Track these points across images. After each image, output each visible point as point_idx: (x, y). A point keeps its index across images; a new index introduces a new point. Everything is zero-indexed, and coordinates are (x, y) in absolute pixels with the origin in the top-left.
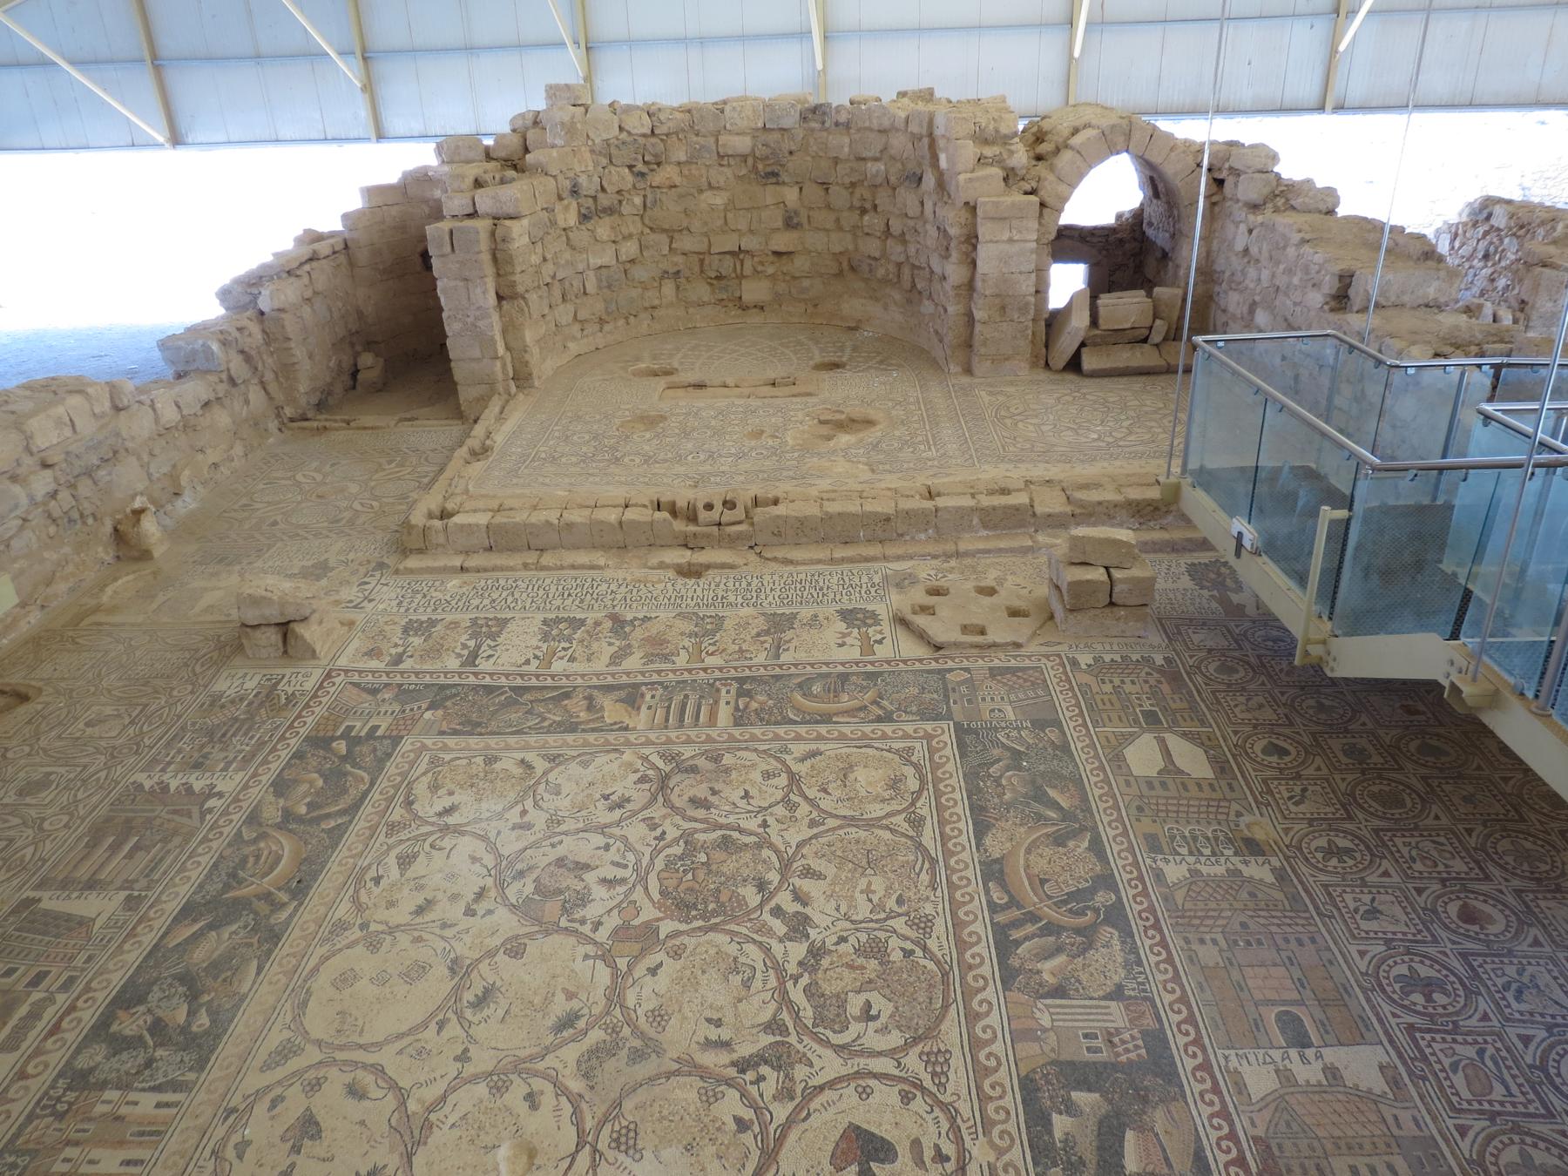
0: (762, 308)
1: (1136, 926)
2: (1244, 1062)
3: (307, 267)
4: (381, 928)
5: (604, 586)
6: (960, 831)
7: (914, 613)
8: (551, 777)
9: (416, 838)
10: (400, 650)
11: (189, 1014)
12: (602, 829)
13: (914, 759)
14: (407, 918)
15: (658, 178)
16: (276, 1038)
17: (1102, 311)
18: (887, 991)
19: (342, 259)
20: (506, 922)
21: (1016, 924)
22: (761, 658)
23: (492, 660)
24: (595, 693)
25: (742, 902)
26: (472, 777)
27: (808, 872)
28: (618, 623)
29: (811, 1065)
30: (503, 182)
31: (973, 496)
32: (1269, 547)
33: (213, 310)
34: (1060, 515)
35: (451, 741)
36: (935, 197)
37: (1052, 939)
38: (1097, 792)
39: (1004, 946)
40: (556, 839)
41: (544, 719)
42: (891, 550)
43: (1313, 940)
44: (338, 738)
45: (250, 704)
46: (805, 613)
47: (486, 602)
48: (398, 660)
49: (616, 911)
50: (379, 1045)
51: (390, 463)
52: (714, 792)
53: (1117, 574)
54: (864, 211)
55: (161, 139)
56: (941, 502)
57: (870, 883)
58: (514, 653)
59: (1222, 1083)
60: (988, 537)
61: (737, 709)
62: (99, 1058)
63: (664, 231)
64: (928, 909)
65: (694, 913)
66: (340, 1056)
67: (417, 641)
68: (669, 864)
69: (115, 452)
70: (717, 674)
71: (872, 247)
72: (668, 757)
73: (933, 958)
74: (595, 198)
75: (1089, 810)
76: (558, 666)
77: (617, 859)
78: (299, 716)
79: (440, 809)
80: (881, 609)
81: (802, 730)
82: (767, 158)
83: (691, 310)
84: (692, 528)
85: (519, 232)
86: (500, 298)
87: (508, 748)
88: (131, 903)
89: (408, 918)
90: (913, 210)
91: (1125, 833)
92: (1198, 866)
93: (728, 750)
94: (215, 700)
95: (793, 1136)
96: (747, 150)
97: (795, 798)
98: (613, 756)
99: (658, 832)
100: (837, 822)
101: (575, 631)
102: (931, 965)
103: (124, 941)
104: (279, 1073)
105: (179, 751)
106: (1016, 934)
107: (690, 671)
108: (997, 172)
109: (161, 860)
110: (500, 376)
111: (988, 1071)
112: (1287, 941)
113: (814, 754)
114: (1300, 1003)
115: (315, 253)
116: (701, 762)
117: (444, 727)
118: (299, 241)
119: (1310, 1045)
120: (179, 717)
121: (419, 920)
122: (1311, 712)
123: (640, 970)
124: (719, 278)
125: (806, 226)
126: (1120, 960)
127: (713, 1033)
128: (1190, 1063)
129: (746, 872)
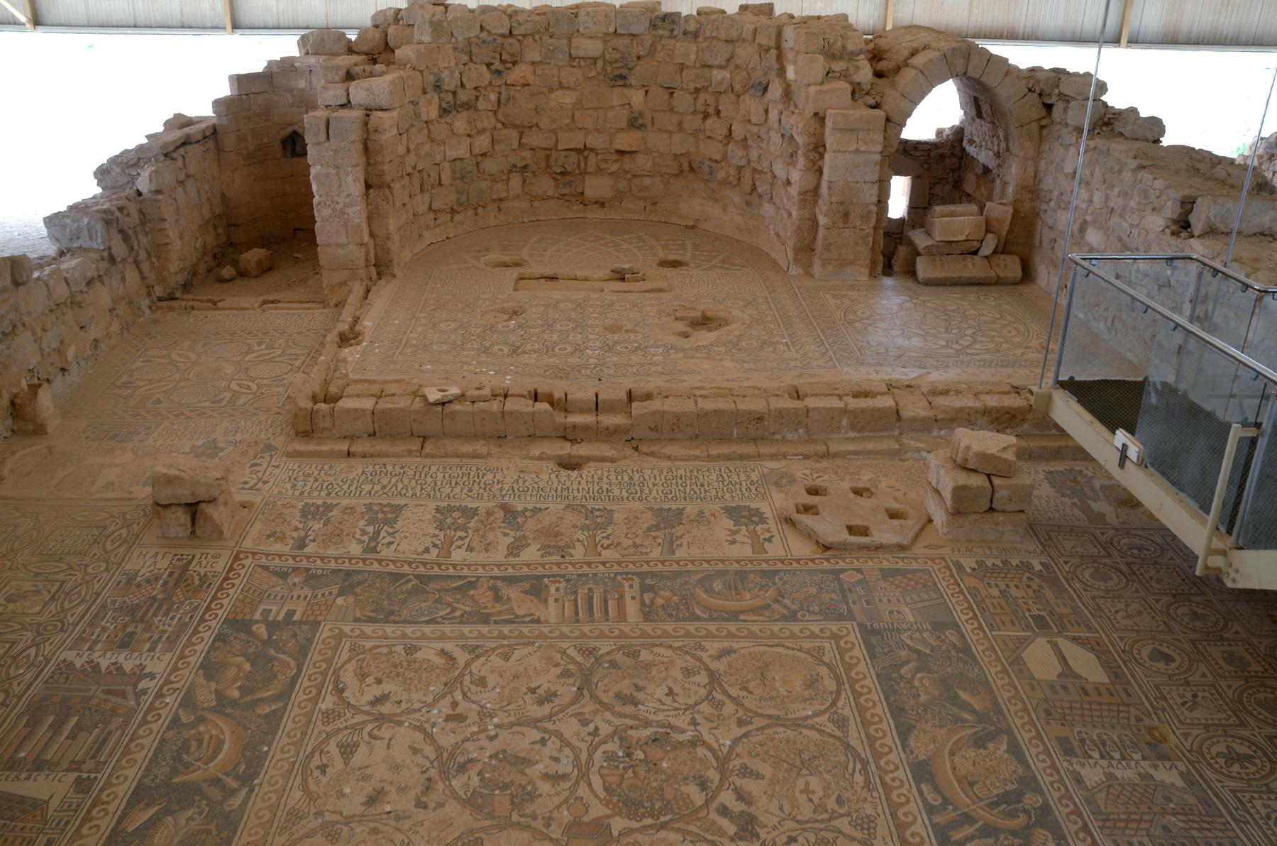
5: (489, 476)
8: (475, 667)
9: (353, 727)
10: (302, 533)
12: (535, 723)
14: (361, 809)
15: (515, 75)
22: (656, 553)
23: (393, 547)
24: (499, 583)
26: (396, 667)
30: (372, 75)
35: (368, 629)
41: (454, 610)
42: (764, 450)
44: (257, 622)
46: (691, 509)
48: (301, 544)
52: (639, 689)
55: (23, 19)
56: (811, 402)
58: (412, 539)
60: (853, 440)
61: (643, 604)
63: (516, 127)
65: (642, 810)
67: (317, 526)
68: (610, 757)
69: (14, 326)
70: (616, 568)
74: (454, 93)
76: (458, 555)
79: (372, 698)
80: (765, 508)
81: (712, 627)
83: (536, 203)
86: (368, 186)
87: (424, 637)
88: (82, 786)
89: (361, 809)
93: (644, 646)
97: (718, 696)
99: (591, 727)
103: (81, 826)
107: (589, 564)
109: (105, 740)
113: (728, 652)
116: (619, 657)
117: (358, 615)
122: (1186, 619)
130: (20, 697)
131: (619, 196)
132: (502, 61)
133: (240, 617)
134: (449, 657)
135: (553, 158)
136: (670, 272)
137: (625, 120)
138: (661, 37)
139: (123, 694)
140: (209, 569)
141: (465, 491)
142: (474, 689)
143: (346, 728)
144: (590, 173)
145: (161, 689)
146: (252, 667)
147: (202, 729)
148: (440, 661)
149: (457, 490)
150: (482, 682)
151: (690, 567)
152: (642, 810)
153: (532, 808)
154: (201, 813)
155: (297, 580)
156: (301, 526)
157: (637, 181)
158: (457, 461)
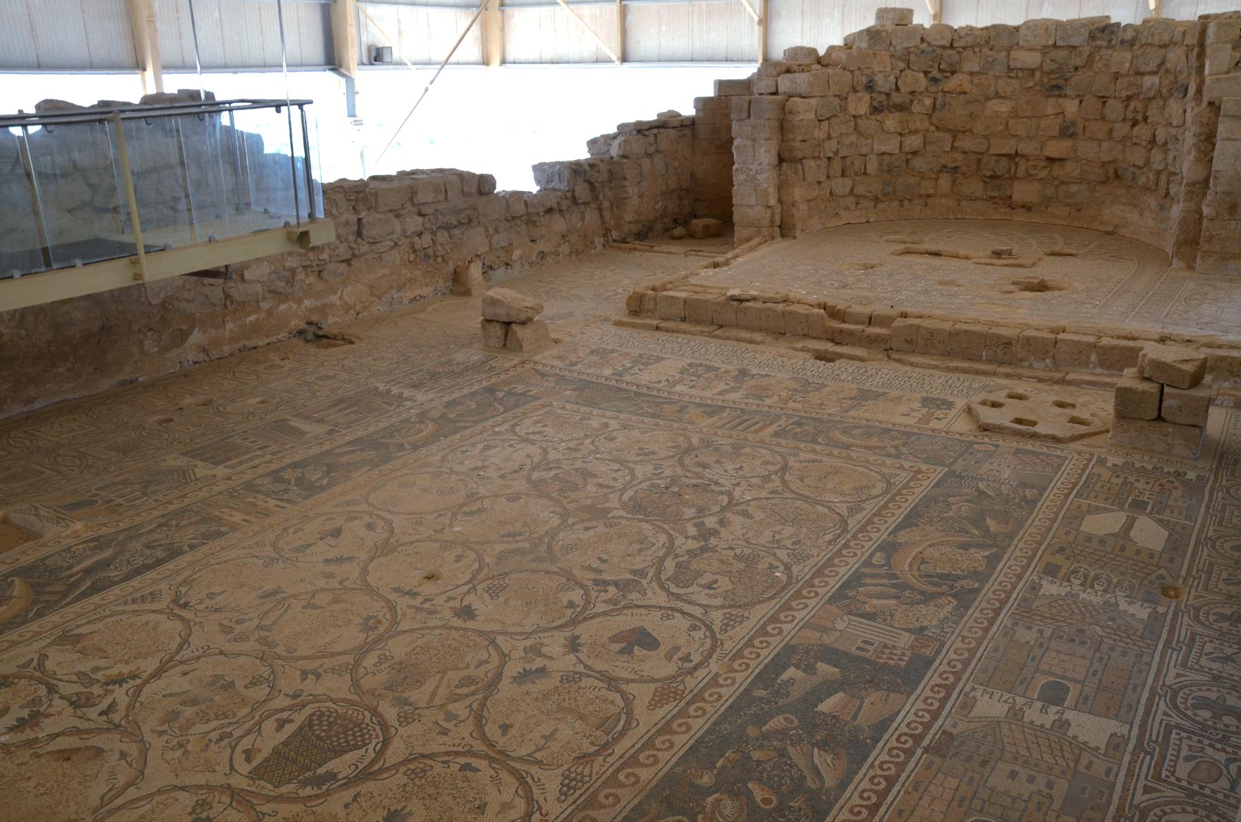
3: (655, 131)
55: (614, 57)
60: (1103, 374)
63: (949, 130)
71: (1136, 156)
82: (1053, 72)
83: (964, 203)
86: (781, 160)
95: (598, 620)
115: (667, 124)
124: (991, 177)
125: (1080, 136)
131: (1047, 201)
132: (940, 70)
135: (984, 162)
137: (1057, 128)
138: (1099, 48)
157: (1064, 187)
158: (735, 343)
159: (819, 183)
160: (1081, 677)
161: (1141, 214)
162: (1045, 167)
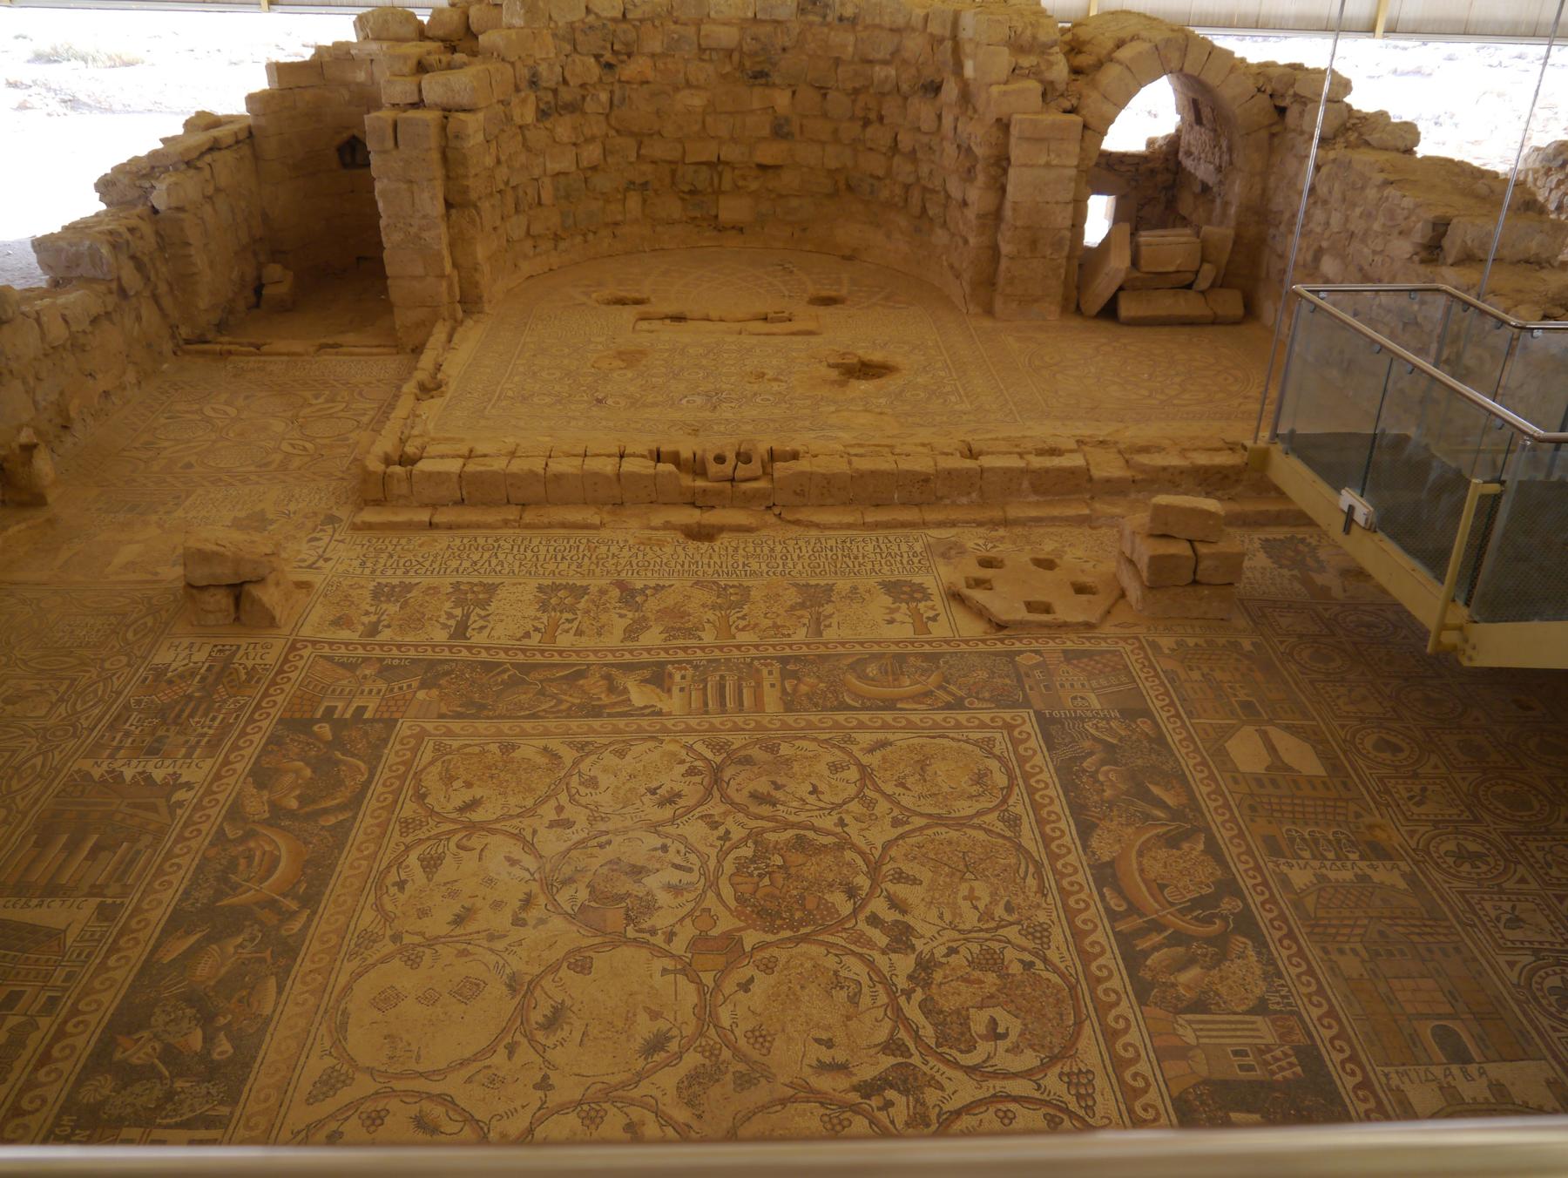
0: (741, 230)
1: (1272, 936)
2: (1405, 1079)
3: (208, 158)
4: (417, 939)
5: (603, 549)
6: (1062, 831)
7: (968, 587)
8: (584, 766)
9: (437, 837)
10: (374, 618)
11: (204, 1038)
12: (654, 828)
13: (997, 751)
14: (444, 929)
15: (630, 70)
16: (316, 1066)
17: (1144, 251)
18: (1012, 1007)
19: (245, 150)
20: (564, 934)
21: (1143, 932)
22: (801, 635)
23: (485, 633)
24: (614, 671)
25: (831, 909)
27: (900, 877)
28: (628, 595)
29: (942, 1088)
30: (450, 67)
31: (1021, 455)
32: (1386, 523)
33: (93, 205)
34: (1120, 480)
35: (456, 726)
36: (956, 111)
37: (1181, 950)
38: (1205, 790)
39: (1133, 960)
40: (603, 839)
41: (560, 702)
42: (931, 516)
43: (1457, 950)
45: (203, 679)
46: (843, 585)
47: (466, 564)
48: (373, 630)
49: (688, 921)
50: (442, 1073)
51: (317, 397)
52: (777, 787)
53: (1203, 549)
54: (867, 123)
56: (986, 461)
57: (972, 889)
58: (509, 621)
59: (1386, 1102)
60: (1037, 504)
61: (784, 690)
62: (106, 1092)
63: (632, 134)
64: (1042, 917)
65: (779, 922)
66: (399, 1085)
67: (393, 608)
68: (741, 866)
70: (753, 652)
71: (876, 164)
72: (718, 747)
73: (1056, 970)
74: (555, 92)
75: (1198, 809)
76: (564, 640)
77: (678, 860)
78: (266, 694)
79: (460, 804)
80: (929, 582)
81: (864, 717)
82: (756, 54)
83: (659, 229)
84: (700, 483)
85: (473, 127)
86: (449, 205)
87: (524, 734)
88: (106, 913)
90: (927, 124)
91: (1241, 835)
92: (1324, 871)
94: (159, 672)
96: (733, 44)
98: (651, 744)
99: (721, 830)
100: (922, 822)
101: (578, 598)
102: (1055, 979)
103: (107, 957)
104: (328, 1106)
105: (127, 734)
106: (1143, 945)
107: (721, 648)
108: (1034, 86)
109: (132, 861)
110: (445, 298)
111: (1138, 1093)
112: (1430, 951)
113: (883, 744)
114: (1453, 1017)
116: (755, 752)
117: (444, 710)
118: (187, 124)
119: (1470, 1061)
120: (119, 693)
121: (459, 931)
123: (729, 986)
124: (692, 192)
126: (1258, 972)
127: (826, 1055)
128: (1350, 1082)
129: (830, 877)
130: (25, 814)
133: (297, 715)
134: (555, 757)
136: (822, 311)
139: (154, 808)
140: (258, 661)
141: (574, 567)
142: (583, 790)
143: (429, 839)
144: (723, 193)
145: (201, 800)
146: (314, 772)
147: (252, 844)
148: (542, 760)
149: (564, 566)
150: (593, 783)
151: (840, 650)
152: (779, 922)
153: (650, 923)
154: (252, 939)
155: (367, 672)
156: (372, 609)
158: (562, 531)
159: (495, 229)
160: (1447, 1009)
161: (888, 236)
162: (756, 178)
